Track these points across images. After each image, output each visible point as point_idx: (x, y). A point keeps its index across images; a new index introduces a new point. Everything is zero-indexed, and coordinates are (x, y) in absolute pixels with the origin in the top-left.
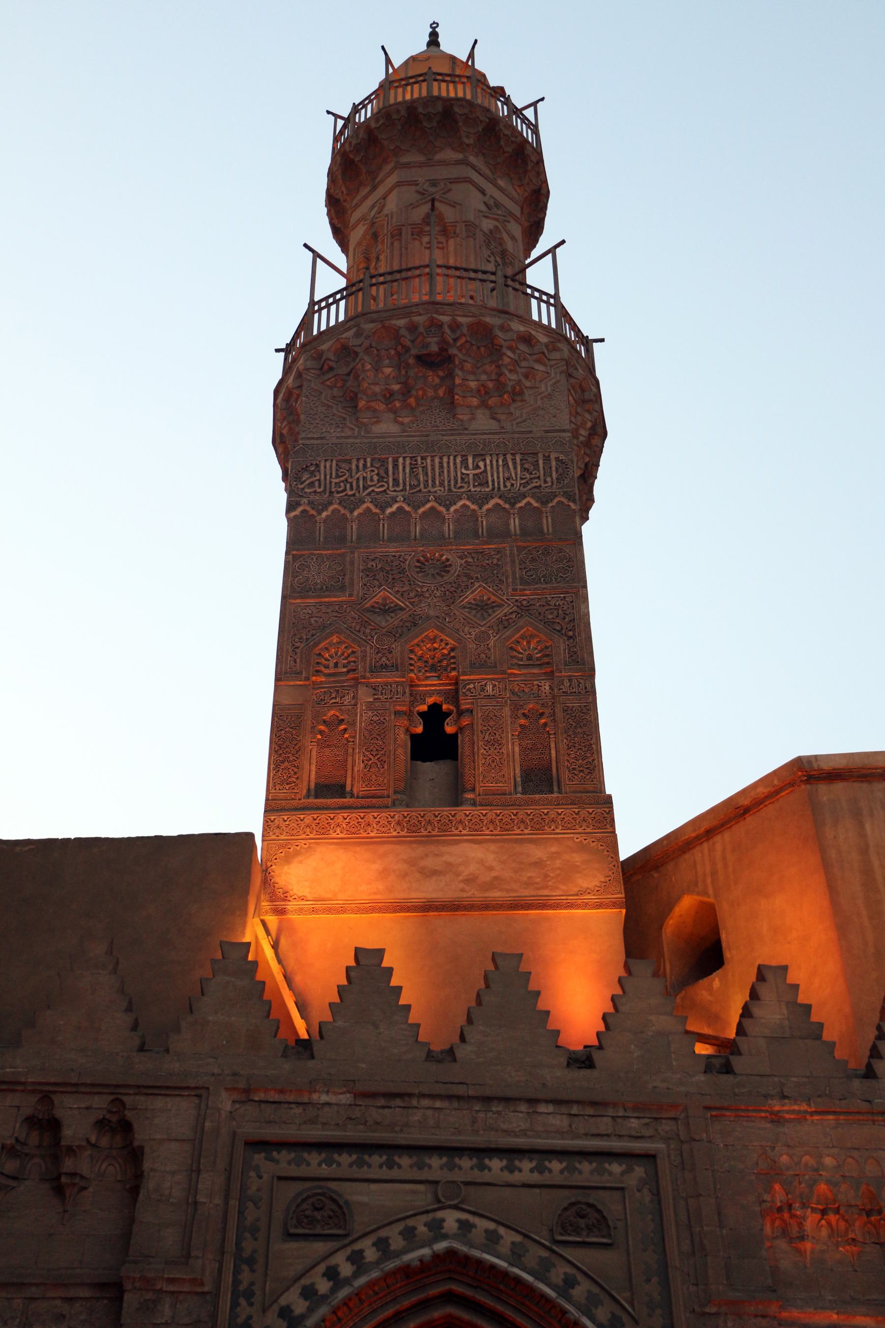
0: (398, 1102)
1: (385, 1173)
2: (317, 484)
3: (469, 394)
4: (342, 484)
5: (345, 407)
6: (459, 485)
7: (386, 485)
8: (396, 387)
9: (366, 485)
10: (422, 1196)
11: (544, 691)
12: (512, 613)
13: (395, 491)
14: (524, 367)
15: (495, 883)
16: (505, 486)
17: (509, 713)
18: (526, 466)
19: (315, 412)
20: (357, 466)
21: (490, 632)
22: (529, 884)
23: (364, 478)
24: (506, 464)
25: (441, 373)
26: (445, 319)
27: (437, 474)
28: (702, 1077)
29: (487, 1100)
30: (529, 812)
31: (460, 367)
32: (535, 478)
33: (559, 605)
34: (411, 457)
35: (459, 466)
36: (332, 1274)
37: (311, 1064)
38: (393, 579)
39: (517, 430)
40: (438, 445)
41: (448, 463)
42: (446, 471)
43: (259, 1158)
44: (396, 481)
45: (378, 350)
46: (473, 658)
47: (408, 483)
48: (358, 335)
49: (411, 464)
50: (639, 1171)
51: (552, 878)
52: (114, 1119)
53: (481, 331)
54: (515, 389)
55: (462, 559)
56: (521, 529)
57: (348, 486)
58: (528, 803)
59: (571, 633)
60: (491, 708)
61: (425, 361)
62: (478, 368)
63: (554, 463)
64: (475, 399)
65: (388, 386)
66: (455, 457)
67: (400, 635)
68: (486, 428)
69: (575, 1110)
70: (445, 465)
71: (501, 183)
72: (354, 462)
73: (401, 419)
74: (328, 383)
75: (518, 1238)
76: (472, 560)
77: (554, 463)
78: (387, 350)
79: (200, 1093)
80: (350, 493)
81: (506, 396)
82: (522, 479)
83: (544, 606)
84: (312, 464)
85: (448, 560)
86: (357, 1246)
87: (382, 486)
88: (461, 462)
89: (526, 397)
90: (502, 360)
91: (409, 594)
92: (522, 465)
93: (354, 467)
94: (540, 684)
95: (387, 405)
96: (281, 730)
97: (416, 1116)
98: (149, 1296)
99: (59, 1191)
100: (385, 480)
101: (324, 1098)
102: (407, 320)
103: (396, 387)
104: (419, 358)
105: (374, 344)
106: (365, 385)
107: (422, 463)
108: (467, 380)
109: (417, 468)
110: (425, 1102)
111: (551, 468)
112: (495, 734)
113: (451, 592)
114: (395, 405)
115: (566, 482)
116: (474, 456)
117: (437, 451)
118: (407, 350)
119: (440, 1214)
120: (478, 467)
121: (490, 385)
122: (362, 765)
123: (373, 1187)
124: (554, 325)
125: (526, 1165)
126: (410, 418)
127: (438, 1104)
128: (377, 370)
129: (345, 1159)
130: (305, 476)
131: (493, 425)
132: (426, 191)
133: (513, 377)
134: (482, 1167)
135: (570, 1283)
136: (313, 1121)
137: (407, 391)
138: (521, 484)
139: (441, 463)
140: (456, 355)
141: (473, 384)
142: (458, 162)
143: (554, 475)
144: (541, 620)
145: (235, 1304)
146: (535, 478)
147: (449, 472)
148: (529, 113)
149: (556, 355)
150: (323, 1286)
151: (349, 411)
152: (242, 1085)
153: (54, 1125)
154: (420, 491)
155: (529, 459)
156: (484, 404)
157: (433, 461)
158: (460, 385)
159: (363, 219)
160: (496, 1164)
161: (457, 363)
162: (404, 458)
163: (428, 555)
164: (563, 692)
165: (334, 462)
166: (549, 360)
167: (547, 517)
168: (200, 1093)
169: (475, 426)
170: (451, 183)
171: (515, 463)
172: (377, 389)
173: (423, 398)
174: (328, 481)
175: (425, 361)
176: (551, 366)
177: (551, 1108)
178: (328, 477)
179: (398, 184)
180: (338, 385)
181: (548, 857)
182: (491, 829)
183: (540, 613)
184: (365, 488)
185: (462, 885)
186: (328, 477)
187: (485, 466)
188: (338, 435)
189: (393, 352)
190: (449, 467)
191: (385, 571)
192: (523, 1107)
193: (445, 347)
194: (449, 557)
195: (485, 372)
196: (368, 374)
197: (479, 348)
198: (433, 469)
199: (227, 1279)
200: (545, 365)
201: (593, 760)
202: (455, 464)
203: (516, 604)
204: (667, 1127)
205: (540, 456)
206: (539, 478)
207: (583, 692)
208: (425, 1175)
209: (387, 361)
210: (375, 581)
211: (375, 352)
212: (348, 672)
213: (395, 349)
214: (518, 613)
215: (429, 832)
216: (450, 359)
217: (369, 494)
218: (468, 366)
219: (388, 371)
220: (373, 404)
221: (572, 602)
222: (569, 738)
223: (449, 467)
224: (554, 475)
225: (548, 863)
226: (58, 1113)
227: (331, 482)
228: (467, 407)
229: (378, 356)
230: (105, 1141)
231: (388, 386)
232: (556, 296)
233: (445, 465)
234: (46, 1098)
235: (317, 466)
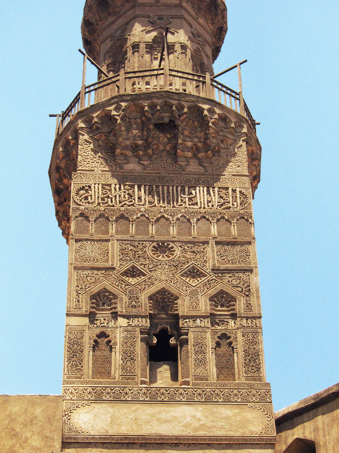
2: (89, 197)
3: (186, 150)
4: (106, 199)
5: (106, 152)
6: (179, 204)
7: (134, 201)
8: (140, 142)
9: (121, 200)
11: (231, 325)
12: (212, 280)
13: (139, 205)
14: (221, 136)
15: (202, 427)
16: (208, 206)
17: (210, 336)
18: (222, 195)
19: (87, 154)
20: (115, 189)
21: (199, 290)
22: (222, 427)
23: (120, 196)
24: (209, 193)
25: (169, 136)
27: (166, 196)
30: (222, 390)
31: (182, 132)
32: (226, 202)
33: (241, 277)
34: (149, 185)
35: (179, 192)
38: (139, 257)
39: (216, 173)
40: (167, 179)
41: (173, 190)
42: (171, 195)
44: (139, 198)
45: (129, 119)
46: (188, 304)
47: (147, 201)
49: (149, 189)
51: (235, 426)
54: (215, 148)
55: (182, 248)
56: (218, 232)
57: (110, 200)
59: (247, 293)
60: (199, 333)
62: (192, 134)
63: (238, 195)
64: (190, 153)
65: (135, 142)
66: (177, 187)
67: (144, 289)
68: (196, 170)
70: (171, 191)
72: (113, 186)
73: (143, 162)
74: (95, 137)
76: (187, 248)
77: (238, 195)
78: (135, 119)
80: (111, 204)
81: (209, 152)
82: (218, 202)
83: (231, 277)
84: (86, 186)
85: (172, 247)
87: (131, 201)
88: (181, 190)
89: (222, 154)
90: (209, 130)
91: (148, 266)
92: (219, 194)
93: (113, 189)
94: (228, 321)
95: (134, 153)
96: (71, 340)
100: (133, 198)
102: (150, 101)
103: (140, 142)
105: (127, 115)
106: (121, 140)
107: (156, 189)
108: (185, 141)
109: (153, 192)
111: (236, 197)
112: (202, 347)
113: (175, 266)
114: (139, 153)
115: (246, 205)
116: (189, 188)
117: (166, 183)
118: (149, 119)
120: (191, 194)
121: (200, 145)
122: (121, 362)
126: (148, 162)
128: (128, 131)
130: (82, 192)
131: (201, 170)
132: (156, 22)
133: (214, 141)
137: (147, 145)
138: (218, 206)
139: (168, 190)
140: (180, 125)
141: (189, 144)
143: (239, 201)
144: (230, 285)
146: (226, 202)
147: (173, 195)
151: (110, 155)
154: (155, 206)
155: (223, 191)
156: (195, 156)
157: (163, 188)
158: (181, 144)
159: (112, 36)
161: (180, 130)
162: (145, 186)
163: (161, 244)
164: (243, 326)
165: (100, 185)
166: (236, 132)
167: (234, 226)
169: (189, 169)
170: (171, 18)
171: (214, 193)
173: (156, 149)
174: (97, 197)
176: (237, 136)
178: (97, 194)
180: (103, 139)
181: (233, 415)
182: (199, 399)
183: (229, 281)
184: (120, 202)
185: (182, 428)
186: (97, 194)
187: (196, 193)
188: (103, 169)
189: (139, 121)
190: (173, 192)
191: (134, 252)
193: (173, 119)
194: (174, 246)
195: (197, 137)
196: (123, 133)
197: (194, 122)
198: (163, 193)
200: (234, 135)
201: (260, 364)
202: (177, 191)
203: (215, 275)
205: (230, 190)
206: (229, 202)
207: (255, 327)
209: (135, 126)
210: (128, 258)
211: (128, 120)
212: (111, 309)
213: (141, 119)
214: (216, 281)
215: (163, 399)
216: (176, 127)
217: (123, 206)
218: (186, 133)
219: (135, 132)
220: (125, 152)
221: (249, 276)
222: (246, 351)
223: (173, 192)
224: (239, 201)
225: (233, 418)
227: (98, 197)
228: (184, 157)
229: (129, 122)
231: (135, 142)
233: (171, 191)
235: (90, 187)
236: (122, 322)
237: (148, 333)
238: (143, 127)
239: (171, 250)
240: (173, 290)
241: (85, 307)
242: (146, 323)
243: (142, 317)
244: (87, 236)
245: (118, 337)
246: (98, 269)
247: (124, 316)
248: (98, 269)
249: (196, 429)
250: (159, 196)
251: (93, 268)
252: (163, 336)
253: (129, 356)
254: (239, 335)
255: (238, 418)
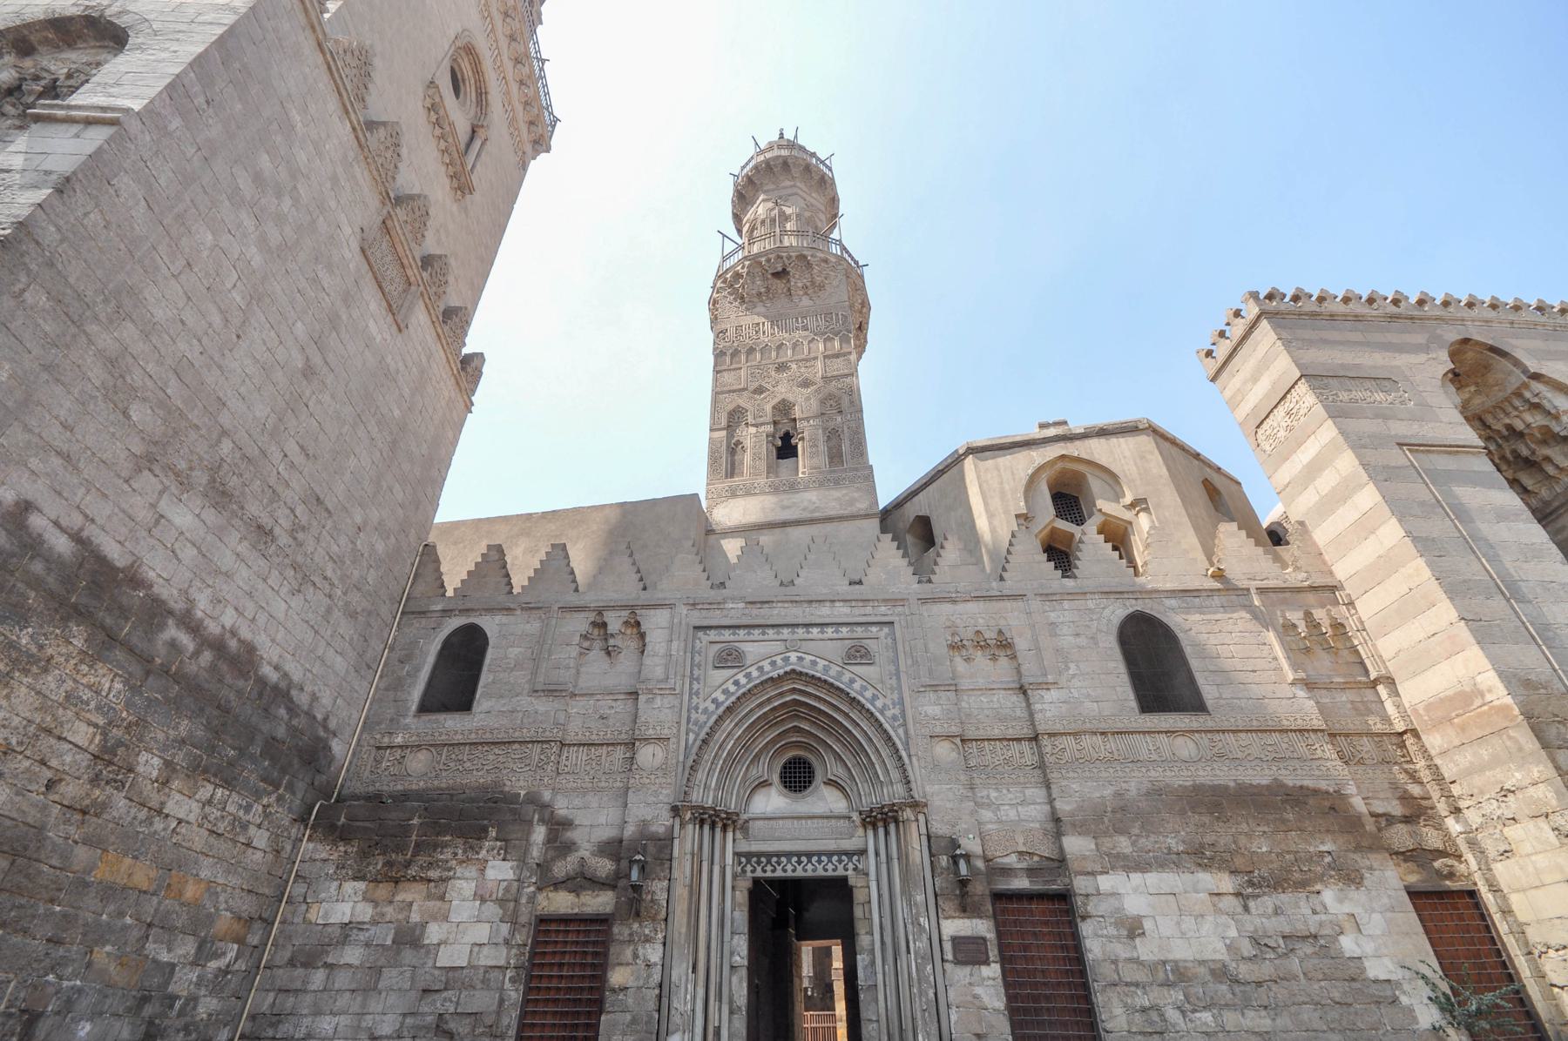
0: (767, 605)
1: (761, 637)
10: (779, 647)
24: (817, 320)
26: (784, 254)
28: (917, 585)
29: (811, 602)
36: (736, 683)
37: (724, 591)
43: (700, 634)
44: (764, 332)
48: (743, 268)
50: (886, 630)
52: (632, 621)
53: (802, 257)
58: (834, 471)
61: (776, 275)
69: (853, 604)
71: (813, 195)
75: (827, 663)
79: (671, 606)
86: (748, 671)
97: (775, 612)
98: (651, 696)
99: (609, 653)
101: (731, 606)
103: (763, 290)
104: (773, 274)
110: (780, 605)
119: (788, 654)
121: (808, 284)
123: (756, 644)
124: (839, 253)
125: (830, 630)
127: (786, 605)
129: (742, 632)
134: (808, 632)
135: (852, 681)
136: (726, 616)
141: (800, 285)
142: (791, 186)
145: (690, 698)
148: (827, 162)
149: (839, 267)
150: (732, 688)
152: (691, 602)
153: (604, 625)
156: (806, 294)
160: (815, 630)
168: (671, 606)
172: (754, 292)
175: (776, 275)
177: (841, 604)
179: (763, 200)
192: (828, 604)
199: (687, 686)
204: (900, 609)
208: (781, 637)
216: (788, 273)
218: (797, 276)
226: (606, 620)
230: (629, 631)
232: (840, 241)
234: (600, 613)
236: (752, 430)
237: (774, 436)
238: (764, 279)
239: (789, 368)
240: (791, 399)
241: (724, 423)
242: (770, 428)
243: (768, 424)
244: (726, 367)
245: (748, 443)
246: (734, 391)
247: (752, 425)
248: (734, 391)
249: (813, 511)
250: (778, 326)
251: (730, 391)
252: (787, 437)
253: (756, 457)
254: (845, 429)
255: (847, 498)
